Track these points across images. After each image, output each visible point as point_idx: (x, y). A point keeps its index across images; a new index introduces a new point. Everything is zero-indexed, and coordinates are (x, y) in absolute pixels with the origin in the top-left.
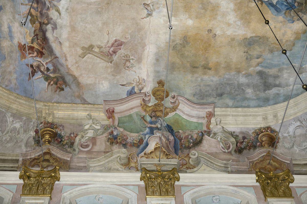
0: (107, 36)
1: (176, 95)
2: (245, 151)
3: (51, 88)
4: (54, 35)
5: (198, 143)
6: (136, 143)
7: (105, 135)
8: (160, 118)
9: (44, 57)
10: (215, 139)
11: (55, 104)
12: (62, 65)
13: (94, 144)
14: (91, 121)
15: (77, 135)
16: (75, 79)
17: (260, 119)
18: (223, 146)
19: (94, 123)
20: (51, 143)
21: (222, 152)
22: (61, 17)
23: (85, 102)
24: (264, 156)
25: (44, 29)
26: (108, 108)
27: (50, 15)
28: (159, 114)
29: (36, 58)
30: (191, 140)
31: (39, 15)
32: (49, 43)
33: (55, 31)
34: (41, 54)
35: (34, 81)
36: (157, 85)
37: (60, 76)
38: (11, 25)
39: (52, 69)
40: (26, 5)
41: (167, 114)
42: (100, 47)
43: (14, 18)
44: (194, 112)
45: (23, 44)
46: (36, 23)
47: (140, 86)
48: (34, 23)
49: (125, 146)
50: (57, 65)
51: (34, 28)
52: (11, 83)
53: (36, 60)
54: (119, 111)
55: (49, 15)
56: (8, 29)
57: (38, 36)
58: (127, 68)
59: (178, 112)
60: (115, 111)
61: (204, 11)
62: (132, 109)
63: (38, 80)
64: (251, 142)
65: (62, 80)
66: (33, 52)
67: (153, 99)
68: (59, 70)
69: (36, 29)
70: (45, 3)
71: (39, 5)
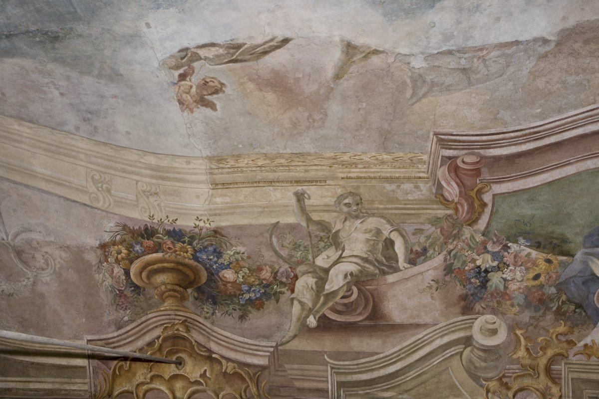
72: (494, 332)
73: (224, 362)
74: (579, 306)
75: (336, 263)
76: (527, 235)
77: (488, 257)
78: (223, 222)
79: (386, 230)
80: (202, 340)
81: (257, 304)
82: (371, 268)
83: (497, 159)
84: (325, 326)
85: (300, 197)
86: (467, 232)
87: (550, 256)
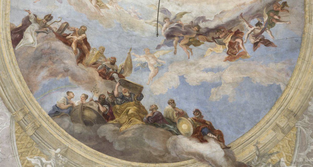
3: (283, 17)
4: (212, 20)
9: (242, 30)
11: (307, 9)
12: (251, 9)
22: (190, 12)
25: (205, 31)
27: (187, 24)
29: (243, 40)
31: (187, 36)
32: (223, 25)
33: (207, 19)
34: (238, 34)
35: (276, 39)
37: (266, 9)
38: (202, 69)
39: (258, 20)
40: (176, 48)
43: (194, 64)
45: (226, 56)
46: (198, 40)
48: (199, 41)
50: (252, 15)
51: (205, 42)
52: (283, 69)
53: (247, 39)
55: (188, 25)
56: (209, 73)
57: (214, 37)
63: (274, 34)
65: (272, 6)
66: (237, 43)
68: (258, 11)
69: (205, 39)
71: (175, 34)
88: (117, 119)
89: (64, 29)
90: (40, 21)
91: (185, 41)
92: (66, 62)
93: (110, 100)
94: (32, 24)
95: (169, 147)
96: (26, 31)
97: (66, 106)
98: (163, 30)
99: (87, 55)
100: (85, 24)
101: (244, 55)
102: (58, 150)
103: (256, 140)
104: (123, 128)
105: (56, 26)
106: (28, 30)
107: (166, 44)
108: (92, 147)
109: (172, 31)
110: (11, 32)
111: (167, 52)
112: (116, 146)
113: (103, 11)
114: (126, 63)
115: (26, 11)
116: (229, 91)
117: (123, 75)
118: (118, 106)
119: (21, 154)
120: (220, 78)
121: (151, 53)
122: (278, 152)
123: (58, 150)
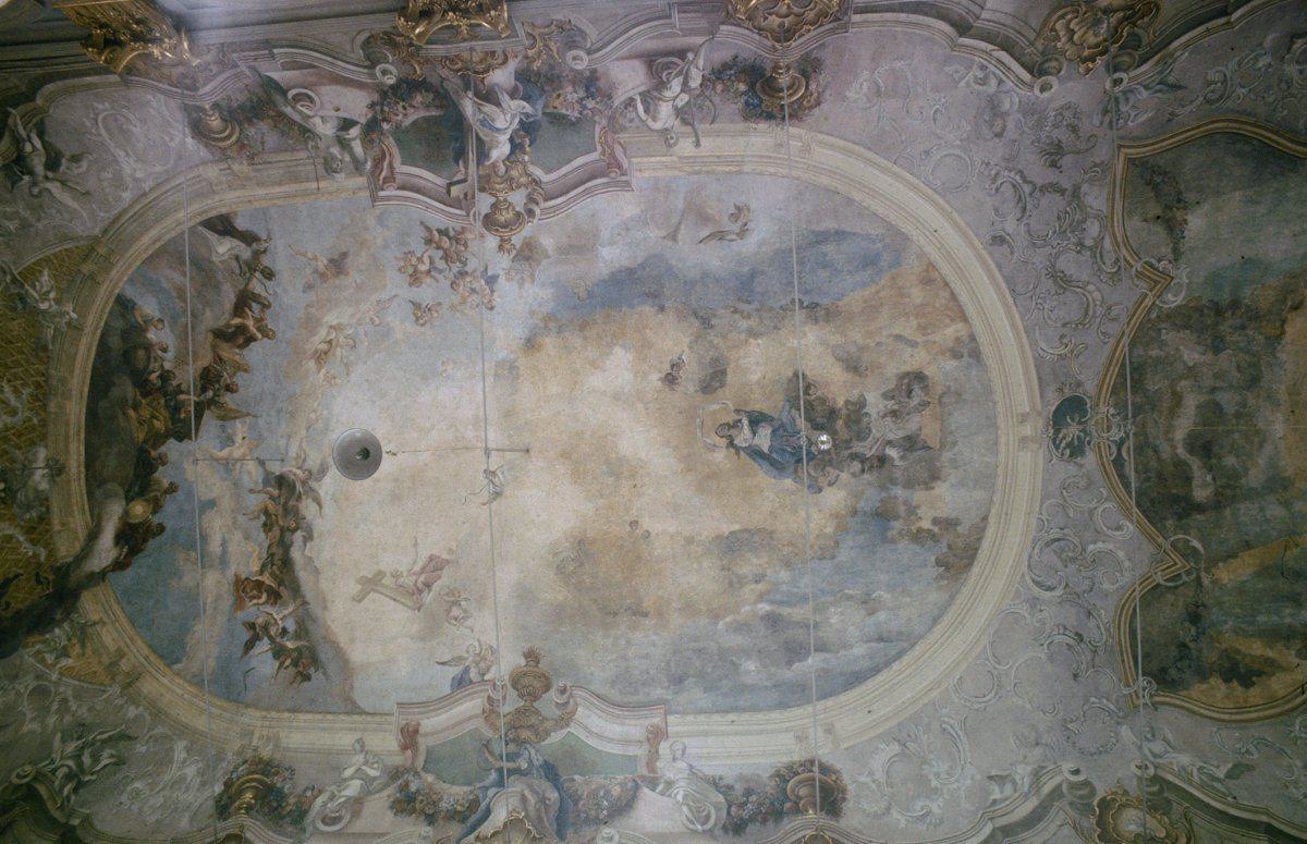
0: (413, 550)
1: (569, 684)
2: (751, 828)
4: (306, 553)
5: (623, 806)
6: (460, 812)
7: (390, 790)
8: (528, 746)
10: (669, 796)
11: (286, 715)
13: (356, 814)
14: (361, 758)
15: (320, 792)
16: (339, 653)
17: (787, 740)
18: (690, 816)
19: (366, 763)
20: (253, 812)
21: (685, 830)
23: (354, 709)
24: (804, 837)
26: (404, 722)
28: (525, 734)
30: (606, 803)
31: (281, 511)
33: (308, 545)
34: (275, 596)
36: (523, 662)
40: (259, 492)
41: (547, 733)
42: (396, 575)
44: (614, 729)
45: (243, 577)
47: (482, 665)
48: (270, 530)
49: (431, 819)
54: (428, 730)
58: (453, 621)
59: (572, 729)
60: (422, 730)
61: (611, 480)
62: (459, 723)
64: (767, 801)
67: (512, 693)
68: (307, 632)
70: (294, 487)
72: (575, 58)
73: (751, 27)
74: (529, 81)
75: (676, 97)
76: (573, 124)
77: (590, 106)
78: (741, 126)
79: (650, 122)
80: (765, 41)
81: (725, 66)
82: (655, 94)
83: (602, 175)
84: (681, 53)
85: (698, 144)
86: (604, 122)
87: (555, 111)
88: (143, 401)
89: (259, 303)
90: (258, 259)
91: (271, 508)
92: (208, 313)
93: (171, 388)
94: (248, 248)
95: (109, 486)
96: (235, 240)
97: (140, 320)
98: (291, 469)
99: (229, 344)
100: (279, 335)
101: (239, 604)
102: (74, 316)
103: (107, 621)
104: (132, 413)
105: (257, 286)
106: (236, 242)
107: (267, 474)
108: (94, 368)
109: (289, 486)
110: (222, 215)
111: (254, 478)
112: (103, 404)
113: (312, 364)
114: (231, 409)
115: (269, 235)
116: (188, 580)
117: (212, 407)
118: (163, 401)
119: (47, 260)
120: (211, 567)
121: (251, 450)
122: (83, 655)
123: (74, 316)
